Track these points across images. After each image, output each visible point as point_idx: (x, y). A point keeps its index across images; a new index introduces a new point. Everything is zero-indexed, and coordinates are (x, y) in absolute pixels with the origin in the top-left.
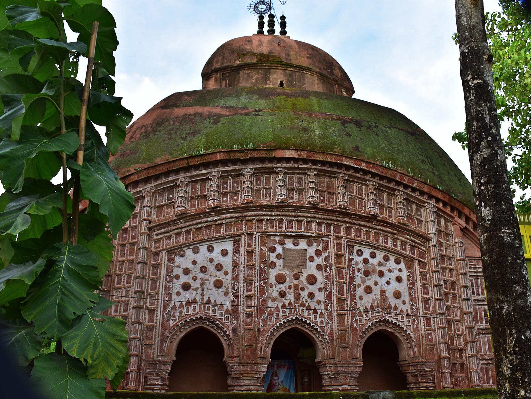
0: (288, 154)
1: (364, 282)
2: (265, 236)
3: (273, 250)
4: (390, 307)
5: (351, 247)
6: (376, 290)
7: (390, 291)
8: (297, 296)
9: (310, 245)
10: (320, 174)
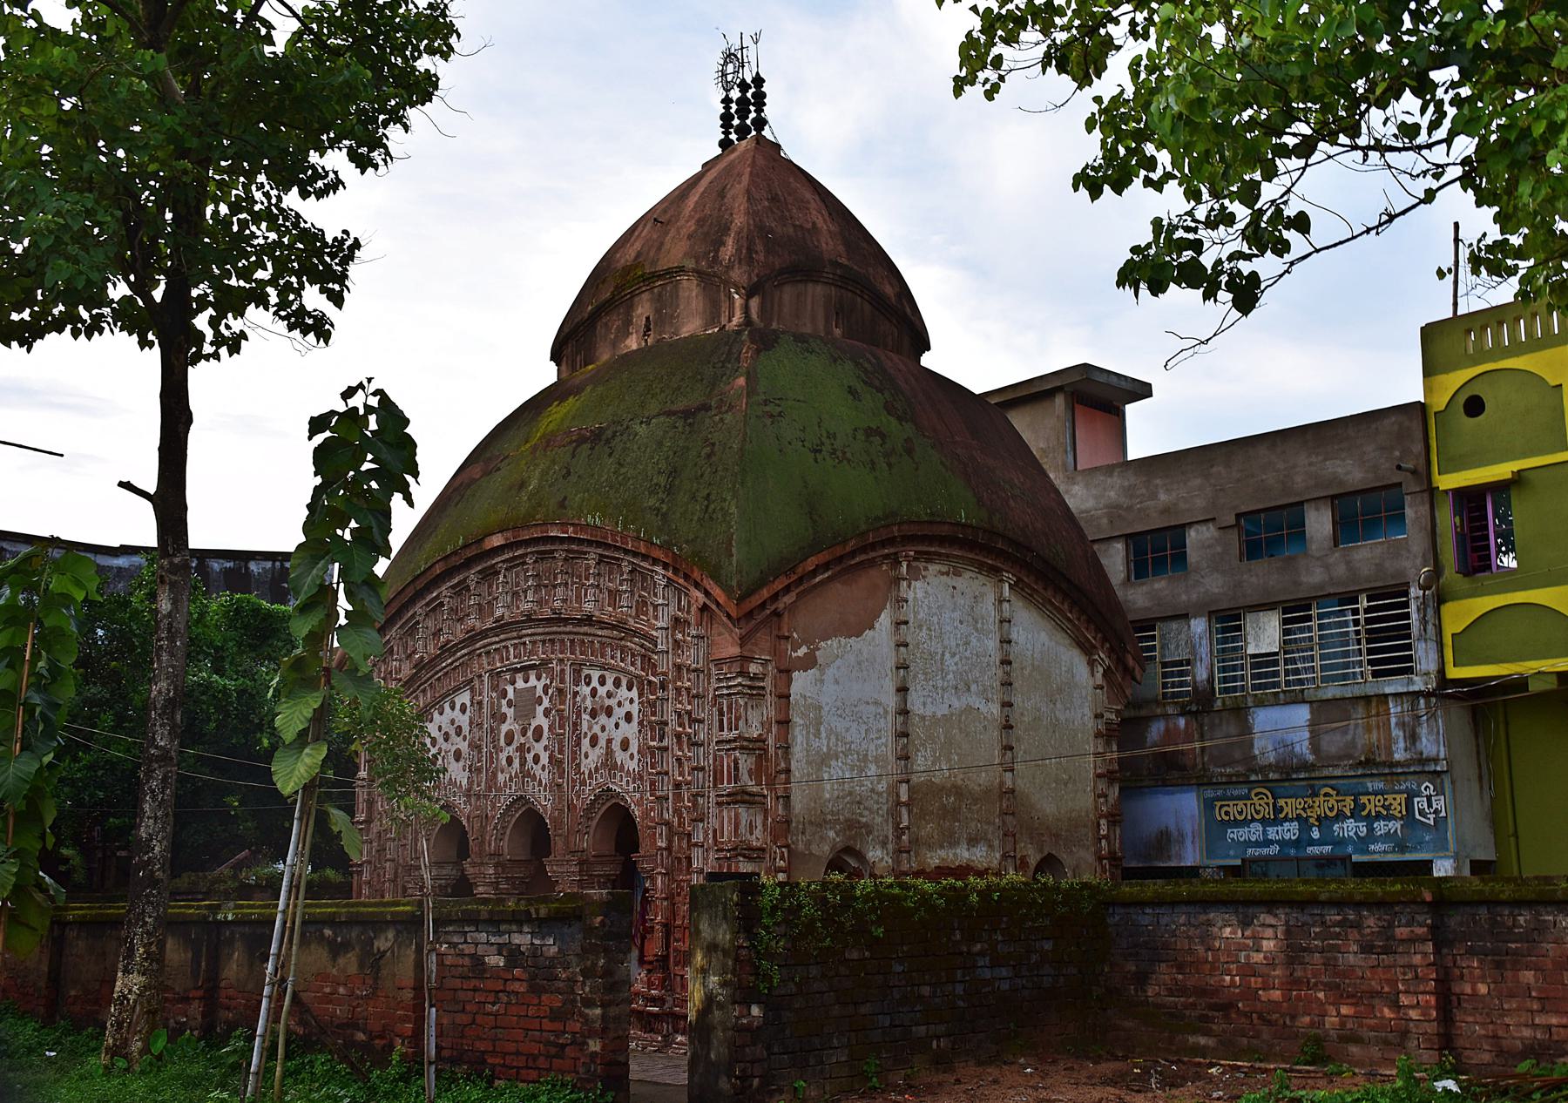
0: (497, 541)
1: (590, 728)
2: (495, 675)
3: (504, 694)
4: (615, 766)
5: (577, 672)
6: (602, 743)
7: (618, 737)
8: (523, 762)
9: (539, 679)
10: (542, 556)
